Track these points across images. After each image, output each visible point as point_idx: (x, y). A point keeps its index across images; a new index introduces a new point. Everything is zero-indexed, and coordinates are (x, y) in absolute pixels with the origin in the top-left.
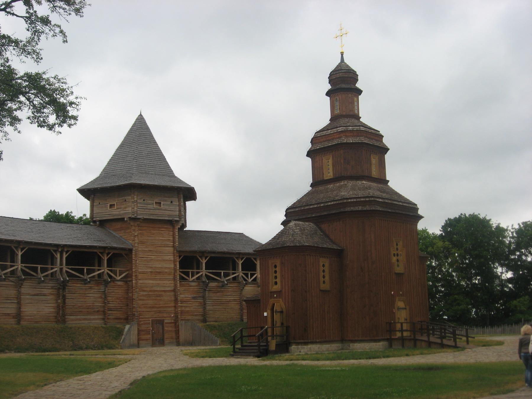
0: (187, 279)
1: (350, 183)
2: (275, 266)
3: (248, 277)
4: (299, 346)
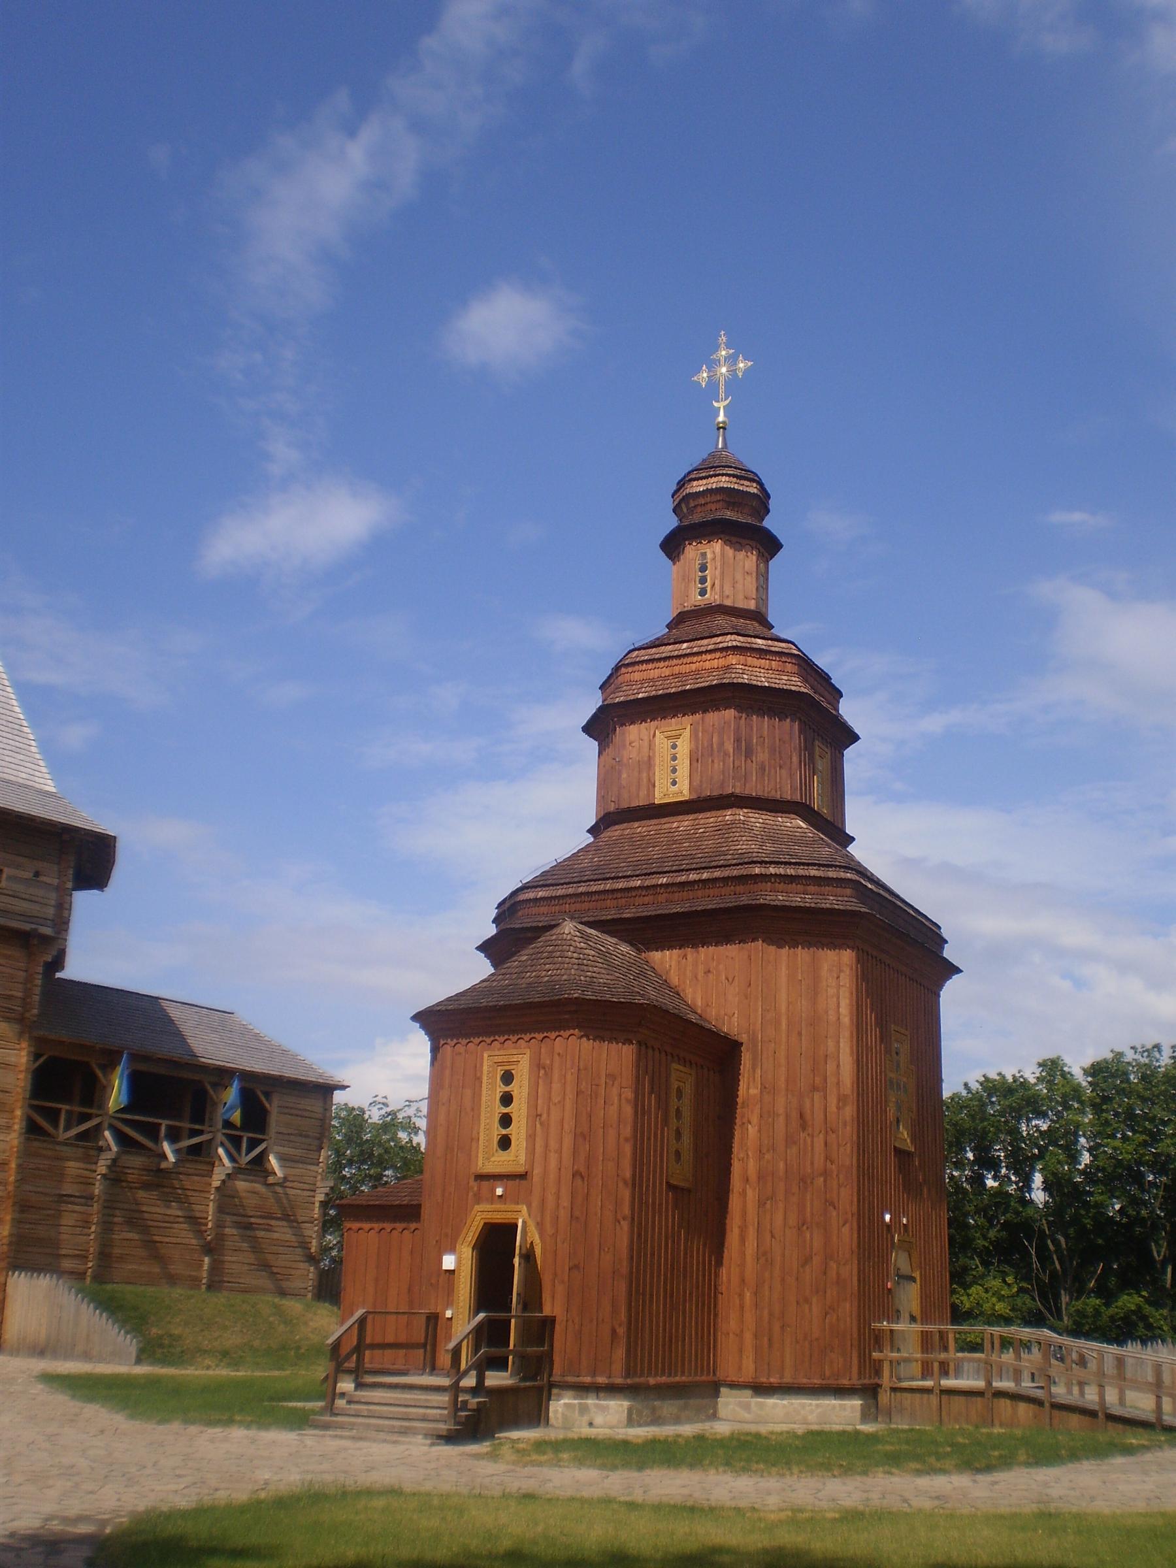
0: (49, 1135)
1: (757, 819)
2: (508, 1078)
3: (238, 1149)
4: (591, 1401)
